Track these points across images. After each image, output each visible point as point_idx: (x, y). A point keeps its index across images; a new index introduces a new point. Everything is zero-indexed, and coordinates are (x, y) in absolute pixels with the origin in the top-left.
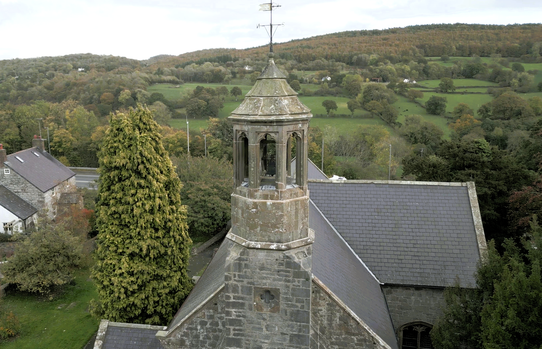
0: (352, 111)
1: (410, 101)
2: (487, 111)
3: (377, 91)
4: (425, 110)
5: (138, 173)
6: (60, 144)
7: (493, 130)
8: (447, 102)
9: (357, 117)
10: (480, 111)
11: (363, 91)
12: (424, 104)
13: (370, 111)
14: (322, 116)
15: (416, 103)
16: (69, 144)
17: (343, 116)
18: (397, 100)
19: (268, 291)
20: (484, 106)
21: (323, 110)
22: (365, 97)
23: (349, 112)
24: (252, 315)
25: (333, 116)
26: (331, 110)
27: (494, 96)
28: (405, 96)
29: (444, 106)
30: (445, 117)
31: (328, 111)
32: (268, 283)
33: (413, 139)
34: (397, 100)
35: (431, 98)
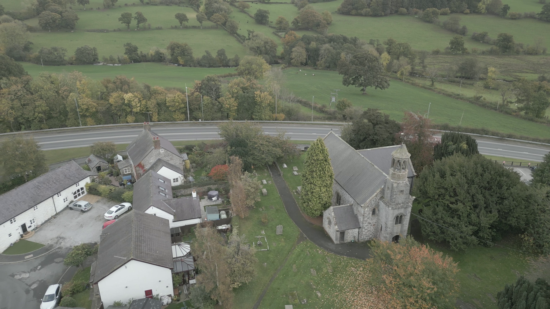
0: (201, 22)
1: (241, 12)
2: (297, 23)
3: (216, 4)
4: (253, 21)
5: (326, 161)
6: (87, 109)
7: (309, 44)
8: (269, 13)
9: (205, 28)
10: (293, 22)
11: (204, 3)
12: (253, 15)
13: (215, 22)
14: (176, 28)
15: (245, 13)
16: (94, 110)
17: (194, 27)
18: (232, 11)
19: (402, 191)
20: (295, 19)
21: (177, 22)
22: (206, 8)
23: (197, 24)
24: (398, 196)
25: (186, 28)
26: (183, 22)
27: (296, 6)
28: (235, 6)
29: (268, 17)
30: (270, 27)
31: (181, 23)
32: (402, 189)
33: (259, 52)
34: (232, 11)
35: (258, 11)
